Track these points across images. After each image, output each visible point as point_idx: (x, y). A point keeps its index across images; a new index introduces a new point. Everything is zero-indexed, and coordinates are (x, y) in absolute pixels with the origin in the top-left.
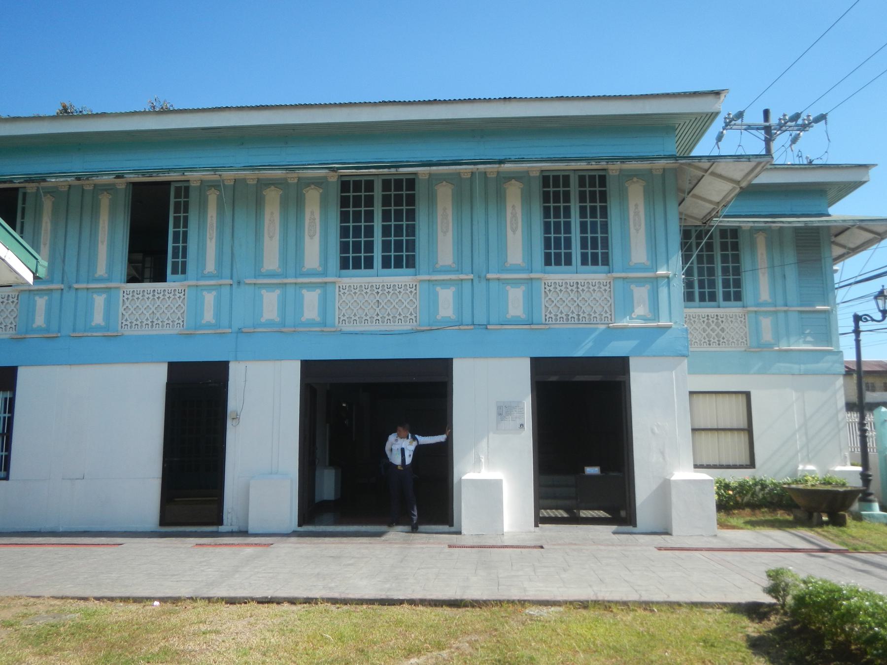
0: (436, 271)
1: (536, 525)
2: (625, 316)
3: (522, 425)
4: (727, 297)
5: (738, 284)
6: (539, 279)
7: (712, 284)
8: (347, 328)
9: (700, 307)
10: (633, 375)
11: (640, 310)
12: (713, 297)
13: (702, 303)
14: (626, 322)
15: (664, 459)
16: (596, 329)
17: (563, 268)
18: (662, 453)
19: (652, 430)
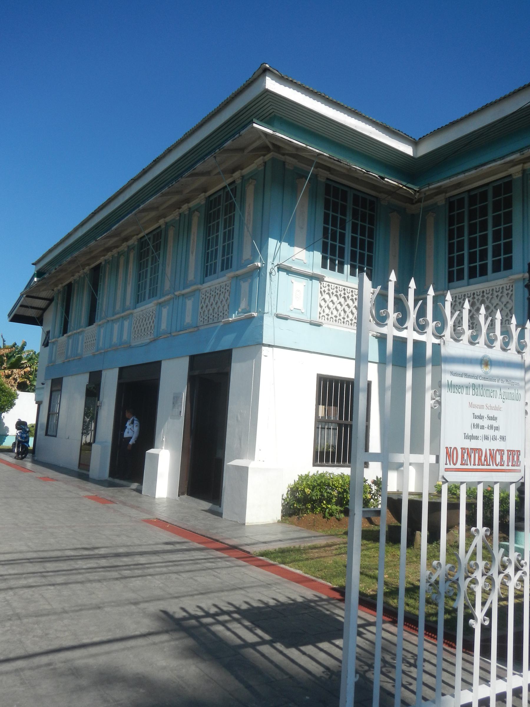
0: (164, 296)
1: (179, 496)
2: (234, 313)
3: (181, 412)
4: (496, 269)
5: (508, 248)
6: (199, 290)
7: (484, 255)
8: (133, 344)
9: (469, 285)
10: (233, 365)
11: (243, 305)
12: (483, 272)
13: (472, 280)
14: (234, 317)
15: (240, 445)
16: (217, 327)
17: (213, 276)
18: (240, 439)
19: (237, 417)
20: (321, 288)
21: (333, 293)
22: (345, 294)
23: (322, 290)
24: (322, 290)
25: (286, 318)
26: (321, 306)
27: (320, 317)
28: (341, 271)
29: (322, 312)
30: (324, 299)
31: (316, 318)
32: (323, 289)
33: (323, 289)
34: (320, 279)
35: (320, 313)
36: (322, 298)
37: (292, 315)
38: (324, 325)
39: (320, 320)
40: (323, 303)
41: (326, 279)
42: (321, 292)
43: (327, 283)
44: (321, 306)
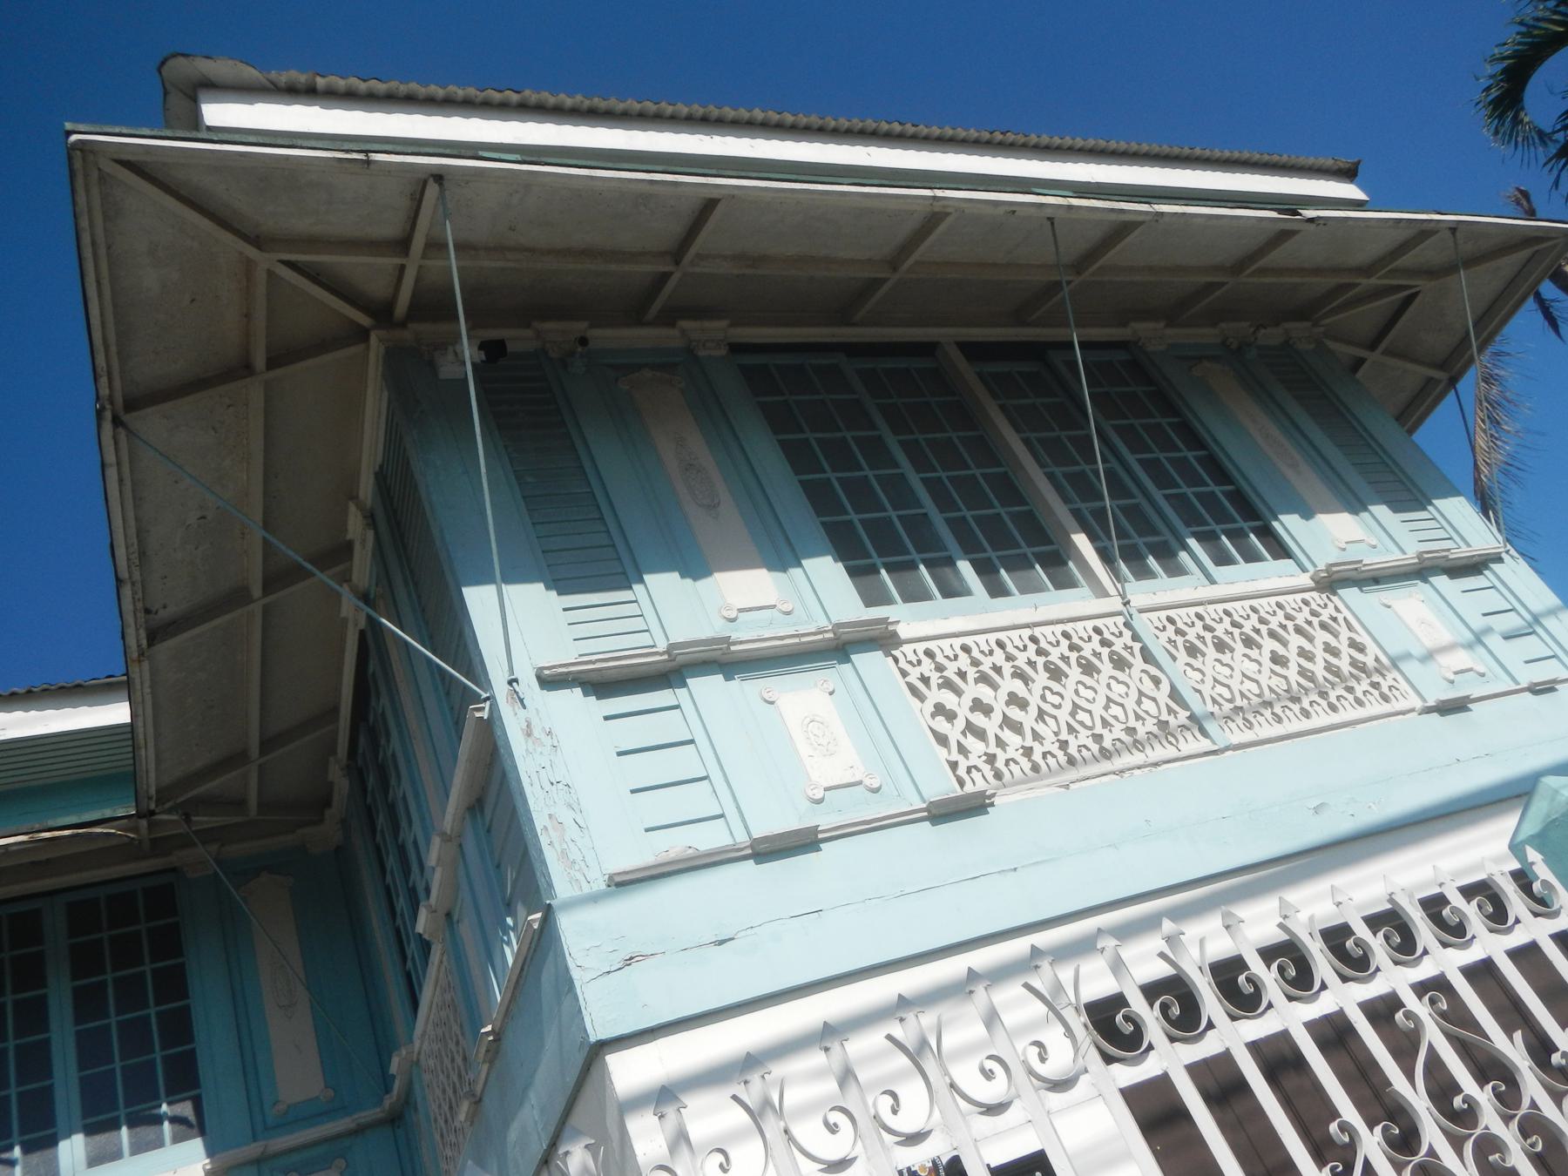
20: (904, 674)
21: (962, 675)
22: (1009, 658)
23: (913, 678)
24: (913, 678)
25: (803, 842)
26: (942, 740)
27: (961, 783)
28: (952, 590)
29: (955, 756)
30: (940, 709)
31: (942, 787)
32: (914, 674)
33: (914, 674)
34: (883, 640)
35: (954, 766)
36: (929, 707)
37: (824, 820)
38: (997, 800)
39: (969, 788)
40: (941, 724)
41: (904, 631)
42: (913, 690)
43: (920, 647)
44: (942, 740)
